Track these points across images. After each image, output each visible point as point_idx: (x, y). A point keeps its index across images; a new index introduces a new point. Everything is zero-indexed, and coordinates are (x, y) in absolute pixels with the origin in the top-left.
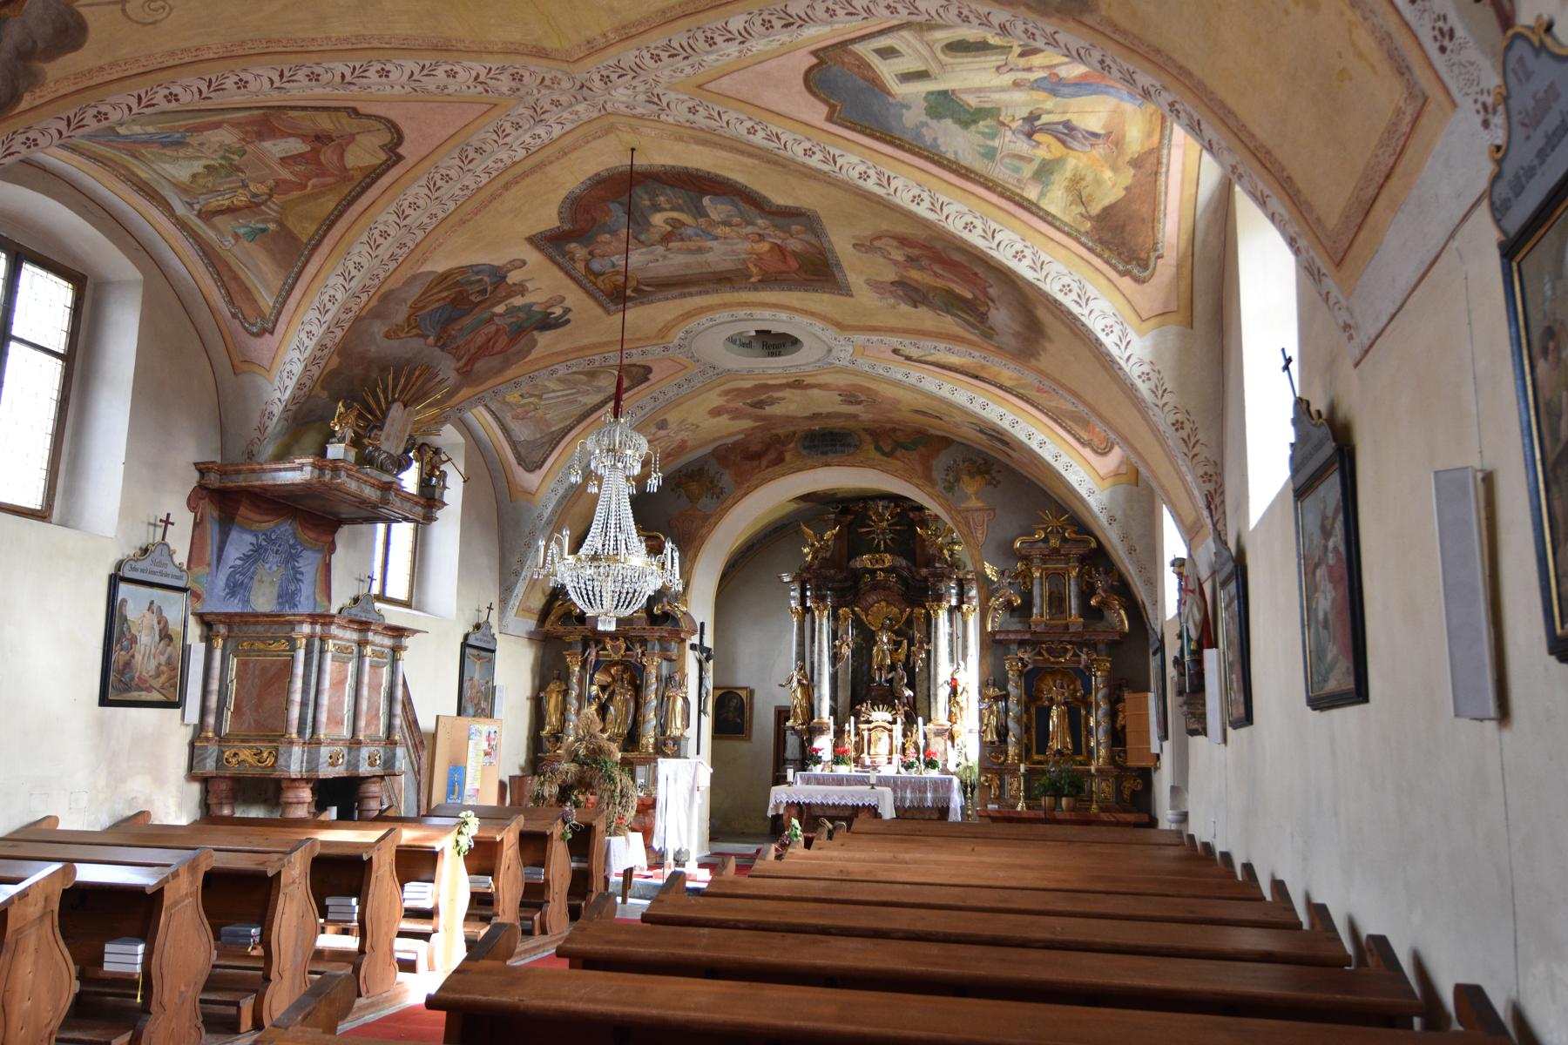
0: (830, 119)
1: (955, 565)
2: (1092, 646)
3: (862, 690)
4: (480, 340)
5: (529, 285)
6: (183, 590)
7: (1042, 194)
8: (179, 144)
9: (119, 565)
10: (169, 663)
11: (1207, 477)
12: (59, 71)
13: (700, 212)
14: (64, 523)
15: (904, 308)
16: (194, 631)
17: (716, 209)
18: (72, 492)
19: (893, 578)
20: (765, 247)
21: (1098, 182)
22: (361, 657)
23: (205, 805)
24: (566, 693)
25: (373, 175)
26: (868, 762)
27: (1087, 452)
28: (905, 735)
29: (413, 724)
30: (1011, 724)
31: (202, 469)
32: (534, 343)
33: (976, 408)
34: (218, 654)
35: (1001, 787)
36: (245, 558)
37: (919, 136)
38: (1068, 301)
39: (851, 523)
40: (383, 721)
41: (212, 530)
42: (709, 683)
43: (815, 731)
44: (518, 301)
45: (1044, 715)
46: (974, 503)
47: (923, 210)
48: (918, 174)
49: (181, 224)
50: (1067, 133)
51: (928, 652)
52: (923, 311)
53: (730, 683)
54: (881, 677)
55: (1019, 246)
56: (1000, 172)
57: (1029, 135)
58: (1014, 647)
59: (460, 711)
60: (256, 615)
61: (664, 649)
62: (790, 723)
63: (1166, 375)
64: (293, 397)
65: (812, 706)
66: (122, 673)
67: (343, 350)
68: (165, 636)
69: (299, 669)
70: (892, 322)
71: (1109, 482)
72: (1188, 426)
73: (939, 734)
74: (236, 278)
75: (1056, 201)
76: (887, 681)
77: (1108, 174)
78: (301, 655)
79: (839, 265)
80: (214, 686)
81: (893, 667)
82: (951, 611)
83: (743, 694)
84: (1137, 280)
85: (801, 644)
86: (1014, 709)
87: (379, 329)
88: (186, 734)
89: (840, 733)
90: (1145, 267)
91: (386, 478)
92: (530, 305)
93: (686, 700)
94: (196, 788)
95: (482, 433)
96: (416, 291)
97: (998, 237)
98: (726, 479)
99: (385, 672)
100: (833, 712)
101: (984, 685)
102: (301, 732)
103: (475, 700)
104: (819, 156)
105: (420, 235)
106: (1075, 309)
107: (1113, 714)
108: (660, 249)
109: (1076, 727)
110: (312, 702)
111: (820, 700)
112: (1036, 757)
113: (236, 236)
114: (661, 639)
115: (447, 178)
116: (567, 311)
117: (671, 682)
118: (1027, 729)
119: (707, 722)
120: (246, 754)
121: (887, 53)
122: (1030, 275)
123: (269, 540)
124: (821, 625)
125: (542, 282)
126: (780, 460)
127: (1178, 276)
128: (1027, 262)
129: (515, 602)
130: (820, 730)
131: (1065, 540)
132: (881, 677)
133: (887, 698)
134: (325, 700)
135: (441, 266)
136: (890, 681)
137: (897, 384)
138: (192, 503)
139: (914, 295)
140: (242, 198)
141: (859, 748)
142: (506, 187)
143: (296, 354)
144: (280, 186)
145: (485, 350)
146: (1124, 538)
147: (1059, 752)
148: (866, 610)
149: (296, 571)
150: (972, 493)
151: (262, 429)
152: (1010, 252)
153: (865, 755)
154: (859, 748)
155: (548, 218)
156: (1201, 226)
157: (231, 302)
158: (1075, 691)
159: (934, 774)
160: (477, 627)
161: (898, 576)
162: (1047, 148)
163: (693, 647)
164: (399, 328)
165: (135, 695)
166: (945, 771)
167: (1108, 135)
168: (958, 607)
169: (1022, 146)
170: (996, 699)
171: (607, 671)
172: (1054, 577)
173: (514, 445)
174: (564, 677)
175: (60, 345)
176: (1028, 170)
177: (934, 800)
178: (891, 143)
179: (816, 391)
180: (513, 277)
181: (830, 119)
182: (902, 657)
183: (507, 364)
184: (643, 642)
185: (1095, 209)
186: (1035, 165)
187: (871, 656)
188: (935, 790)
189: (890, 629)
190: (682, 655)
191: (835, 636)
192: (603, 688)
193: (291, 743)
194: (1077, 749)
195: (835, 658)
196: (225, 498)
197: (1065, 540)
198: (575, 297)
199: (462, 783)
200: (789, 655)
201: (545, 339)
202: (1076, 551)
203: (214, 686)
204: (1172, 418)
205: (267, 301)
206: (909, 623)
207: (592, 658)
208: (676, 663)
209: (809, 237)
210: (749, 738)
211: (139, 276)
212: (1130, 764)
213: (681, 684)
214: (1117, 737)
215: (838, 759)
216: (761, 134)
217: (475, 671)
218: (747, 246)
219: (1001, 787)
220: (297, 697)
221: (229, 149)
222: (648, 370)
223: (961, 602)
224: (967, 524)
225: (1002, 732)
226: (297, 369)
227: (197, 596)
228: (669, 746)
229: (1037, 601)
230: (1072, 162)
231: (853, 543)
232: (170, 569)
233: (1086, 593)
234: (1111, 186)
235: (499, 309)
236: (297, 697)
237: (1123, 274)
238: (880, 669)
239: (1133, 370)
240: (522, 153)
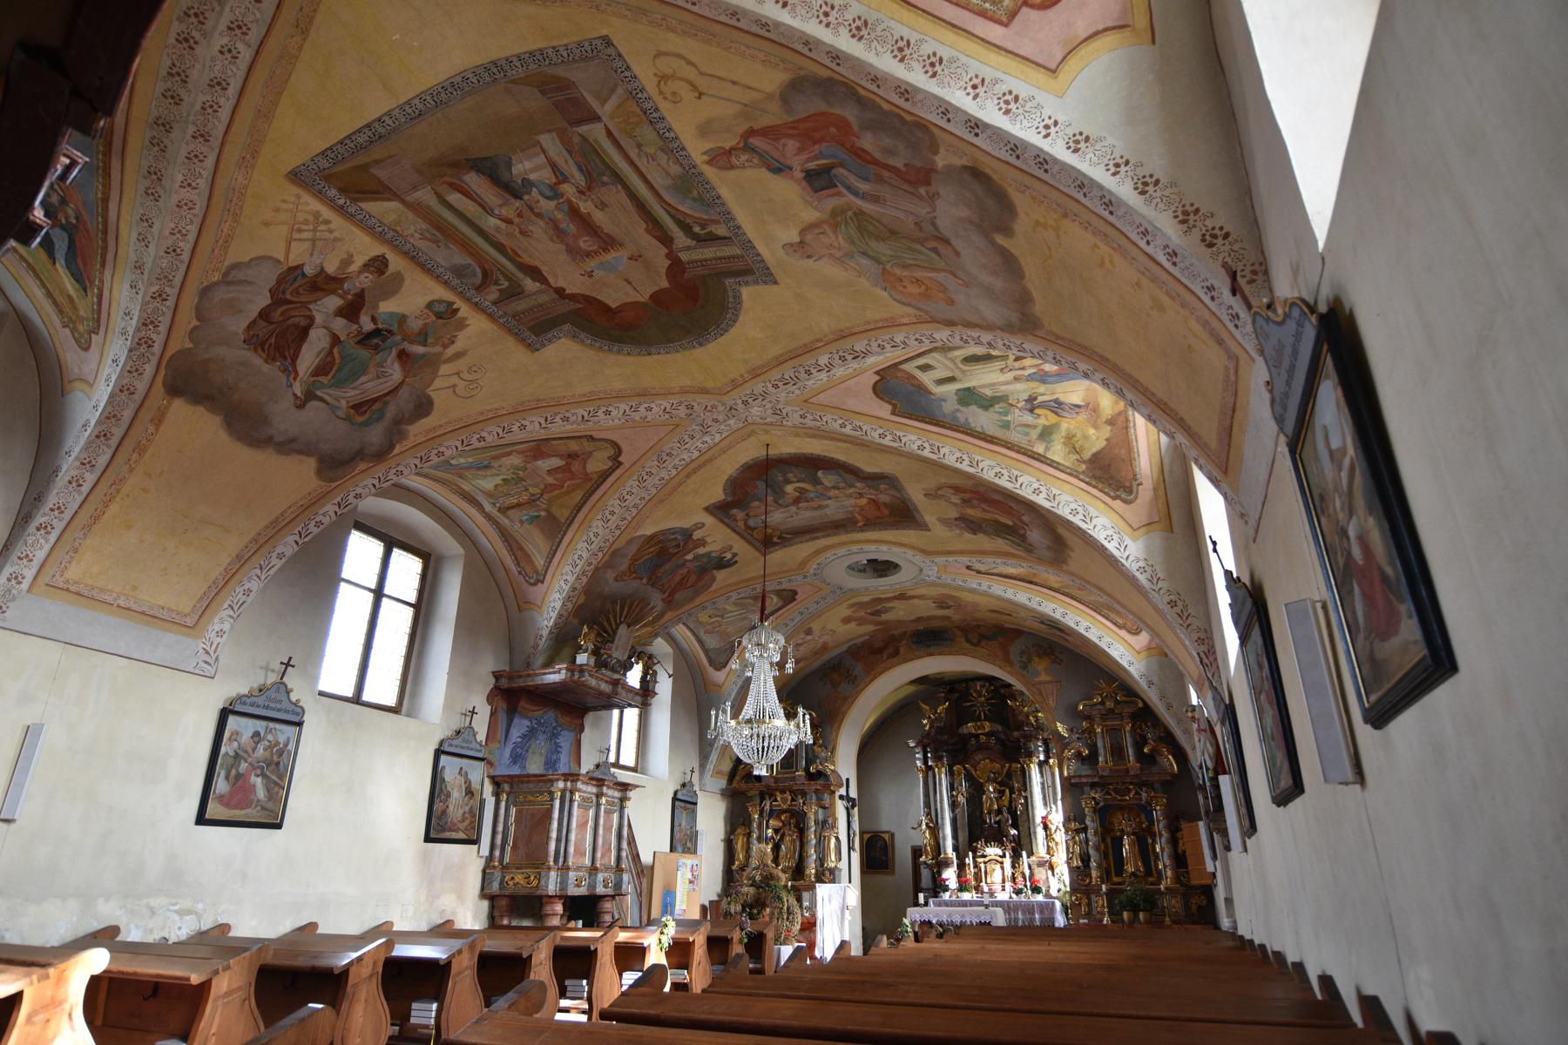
0: (893, 413)
1: (1040, 727)
2: (1150, 786)
3: (978, 830)
4: (678, 578)
5: (708, 540)
6: (482, 759)
7: (1047, 449)
8: (487, 467)
9: (441, 743)
10: (471, 811)
11: (1200, 641)
12: (417, 430)
13: (817, 482)
14: (409, 715)
15: (968, 536)
16: (488, 788)
17: (828, 479)
18: (415, 694)
19: (993, 740)
20: (864, 501)
21: (1086, 437)
22: (598, 805)
23: (492, 917)
24: (749, 835)
25: (605, 476)
26: (986, 889)
27: (1123, 633)
28: (1013, 867)
29: (636, 857)
30: (1091, 852)
31: (497, 675)
32: (714, 579)
33: (1034, 605)
34: (503, 804)
35: (1089, 905)
36: (523, 736)
37: (955, 418)
38: (1077, 520)
40: (614, 853)
41: (502, 717)
42: (856, 826)
44: (701, 551)
45: (1118, 844)
46: (1044, 677)
47: (965, 467)
48: (959, 444)
49: (488, 517)
50: (1057, 407)
51: (1026, 798)
52: (981, 537)
54: (991, 820)
55: (1036, 485)
56: (1015, 437)
57: (1031, 411)
58: (1087, 789)
59: (672, 849)
60: (528, 776)
61: (819, 799)
62: (923, 859)
63: (1158, 568)
64: (556, 624)
66: (439, 818)
67: (588, 591)
68: (469, 792)
69: (556, 815)
70: (961, 547)
71: (1143, 655)
72: (1180, 604)
73: (1041, 864)
74: (521, 548)
75: (1057, 452)
76: (995, 823)
77: (1092, 431)
78: (557, 803)
79: (916, 509)
80: (500, 828)
81: (999, 812)
82: (1041, 764)
83: (886, 837)
84: (1125, 501)
85: (927, 795)
86: (1093, 840)
87: (610, 575)
88: (479, 864)
89: (962, 867)
90: (1130, 492)
91: (616, 676)
92: (709, 554)
93: (837, 838)
94: (486, 904)
95: (685, 646)
96: (634, 548)
97: (1020, 480)
98: (859, 669)
99: (616, 816)
100: (956, 849)
101: (1067, 821)
102: (556, 860)
103: (683, 841)
104: (889, 437)
105: (635, 511)
106: (1083, 526)
107: (1174, 841)
108: (793, 509)
109: (1145, 853)
110: (564, 839)
112: (1116, 879)
113: (522, 522)
114: (816, 791)
115: (650, 474)
116: (735, 555)
117: (826, 824)
118: (1106, 856)
119: (856, 857)
120: (519, 878)
121: (925, 368)
122: (1047, 504)
123: (539, 723)
125: (717, 537)
126: (896, 653)
127: (1156, 497)
128: (1043, 495)
129: (710, 766)
131: (1117, 702)
132: (991, 820)
133: (997, 837)
134: (573, 837)
135: (649, 530)
136: (998, 823)
137: (973, 591)
138: (490, 699)
139: (974, 526)
140: (525, 497)
141: (978, 877)
142: (688, 476)
143: (557, 595)
144: (548, 488)
145: (682, 584)
146: (1162, 697)
147: (1133, 874)
148: (974, 766)
149: (557, 746)
150: (1042, 671)
151: (536, 647)
152: (1030, 490)
154: (978, 877)
155: (717, 494)
156: (1166, 461)
157: (518, 564)
158: (1141, 823)
159: (1040, 898)
160: (684, 785)
161: (998, 739)
162: (1045, 418)
163: (841, 797)
164: (624, 573)
165: (447, 835)
166: (1048, 895)
167: (1087, 405)
168: (1046, 762)
169: (1028, 418)
170: (1077, 831)
171: (778, 818)
172: (1113, 732)
173: (706, 651)
174: (747, 822)
175: (412, 598)
176: (1034, 434)
177: (1042, 920)
178: (936, 425)
179: (916, 601)
180: (697, 535)
181: (893, 413)
183: (697, 594)
184: (804, 794)
185: (1087, 455)
186: (1038, 430)
187: (981, 803)
188: (1042, 912)
189: (994, 781)
190: (833, 804)
191: (952, 787)
192: (776, 831)
193: (549, 868)
194: (1148, 872)
195: (954, 805)
196: (511, 695)
197: (1117, 702)
198: (739, 546)
199: (673, 905)
200: (921, 804)
201: (721, 575)
202: (1127, 710)
203: (500, 828)
204: (1167, 599)
205: (540, 562)
206: (1009, 775)
207: (767, 808)
208: (829, 810)
209: (892, 492)
210: (892, 872)
211: (462, 551)
212: (1194, 882)
213: (834, 826)
214: (1180, 860)
215: (963, 887)
216: (849, 427)
217: (683, 819)
218: (852, 501)
219: (1089, 905)
220: (554, 835)
221: (517, 468)
222: (795, 593)
223: (1048, 757)
224: (1041, 693)
225: (1085, 859)
226: (558, 605)
227: (490, 764)
228: (827, 875)
229: (1101, 751)
230: (1064, 425)
231: (960, 714)
232: (474, 745)
233: (1139, 744)
234: (1096, 439)
235: (689, 557)
236: (554, 835)
237: (1114, 498)
239: (1132, 566)
240: (696, 454)
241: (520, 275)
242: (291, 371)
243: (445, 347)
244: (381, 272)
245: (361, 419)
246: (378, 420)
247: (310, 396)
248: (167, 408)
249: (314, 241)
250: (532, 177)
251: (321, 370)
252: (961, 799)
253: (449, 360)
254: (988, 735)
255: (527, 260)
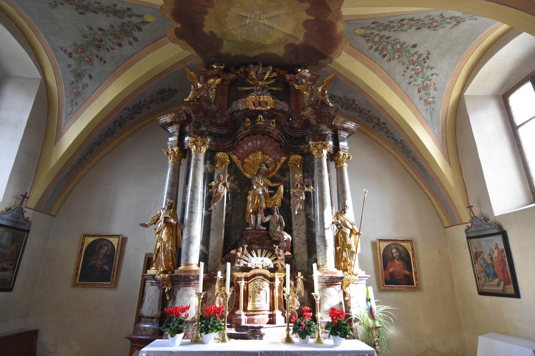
3: (234, 236)
39: (233, 83)
43: (179, 280)
53: (102, 230)
62: (152, 271)
65: (179, 250)
81: (269, 211)
83: (115, 241)
85: (174, 185)
89: (209, 282)
100: (204, 257)
111: (190, 241)
124: (197, 160)
130: (188, 280)
133: (266, 242)
136: (266, 225)
153: (241, 312)
182: (278, 202)
187: (246, 201)
189: (266, 175)
191: (209, 177)
206: (284, 171)
210: (115, 286)
231: (234, 89)
238: (255, 213)
252: (224, 191)
254: (270, 115)
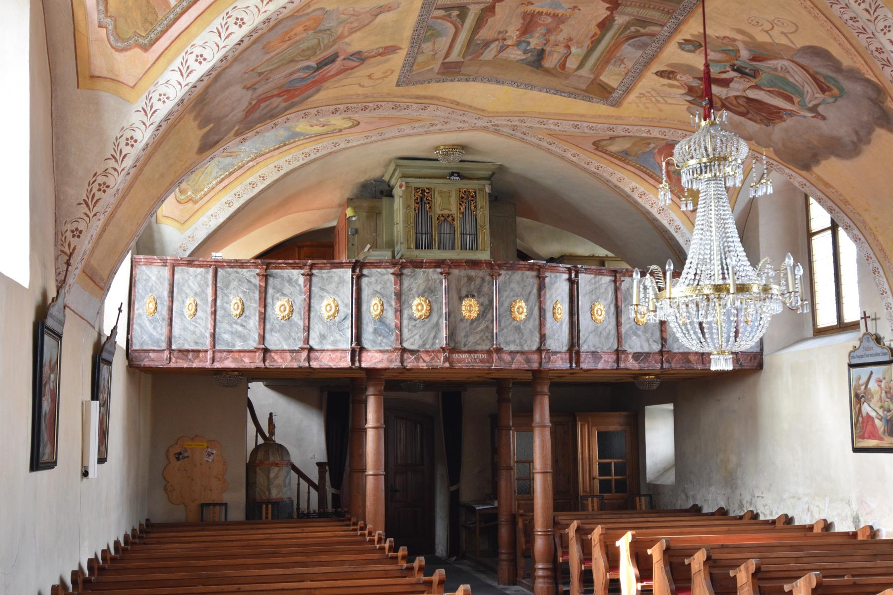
241: (615, 27)
242: (791, 114)
243: (734, 40)
244: (672, 72)
245: (836, 91)
246: (836, 81)
247: (814, 109)
248: (818, 176)
249: (662, 97)
250: (520, 52)
251: (790, 99)
253: (751, 37)
255: (594, 29)
